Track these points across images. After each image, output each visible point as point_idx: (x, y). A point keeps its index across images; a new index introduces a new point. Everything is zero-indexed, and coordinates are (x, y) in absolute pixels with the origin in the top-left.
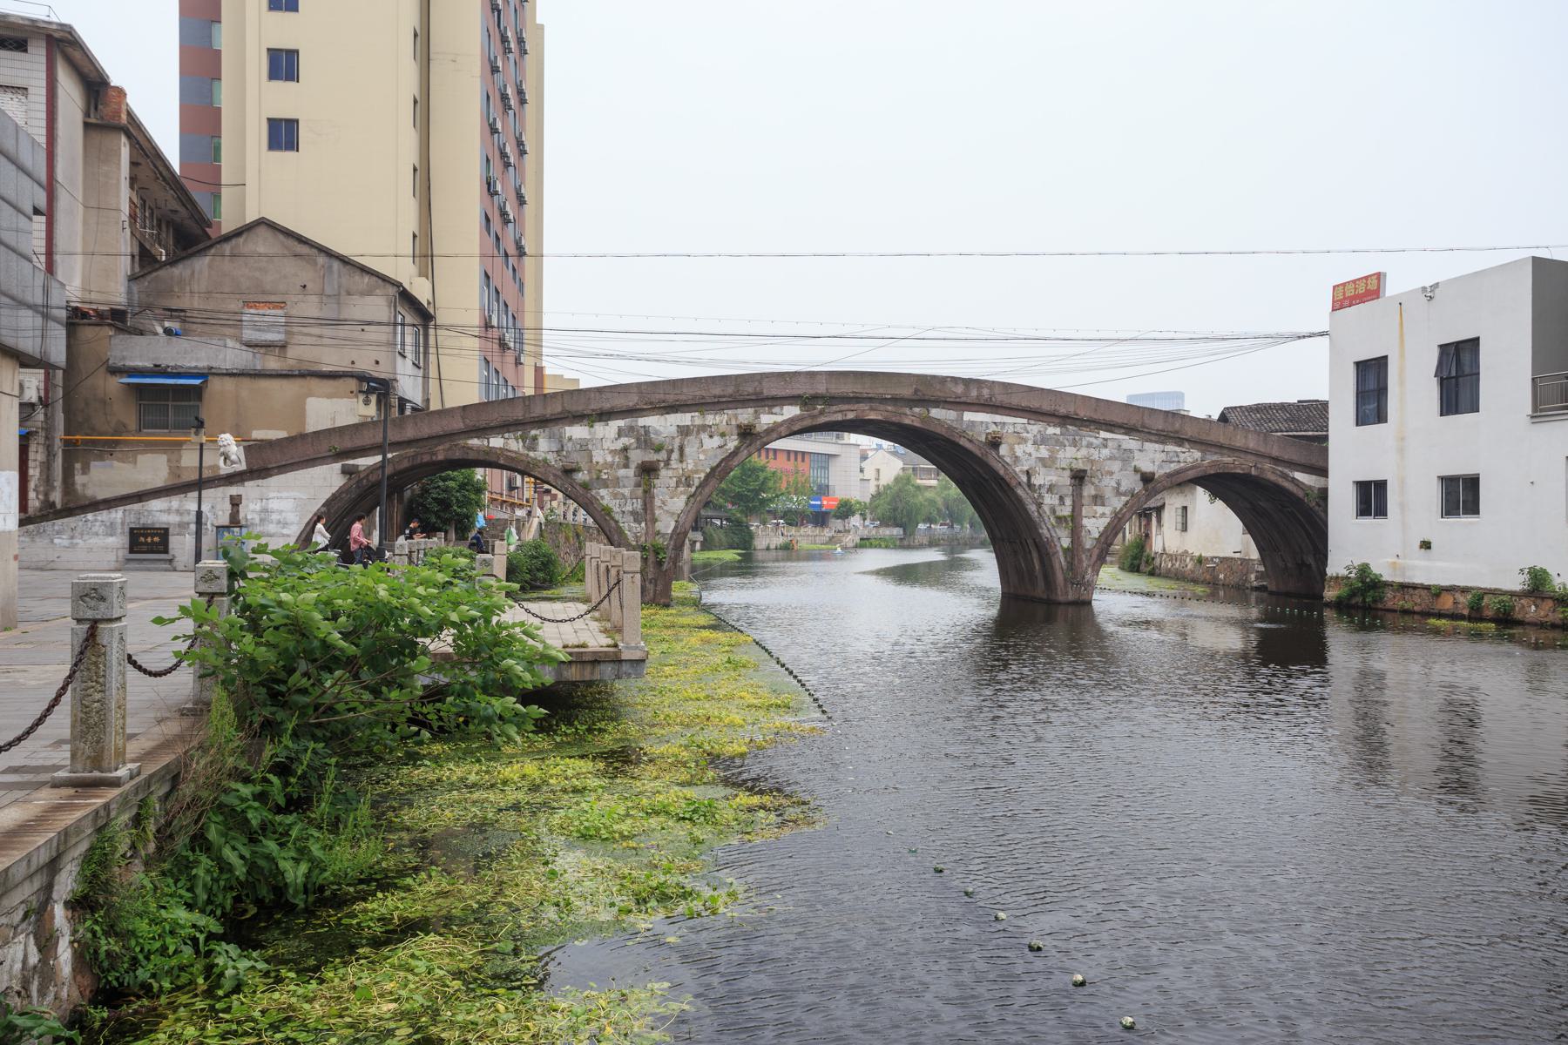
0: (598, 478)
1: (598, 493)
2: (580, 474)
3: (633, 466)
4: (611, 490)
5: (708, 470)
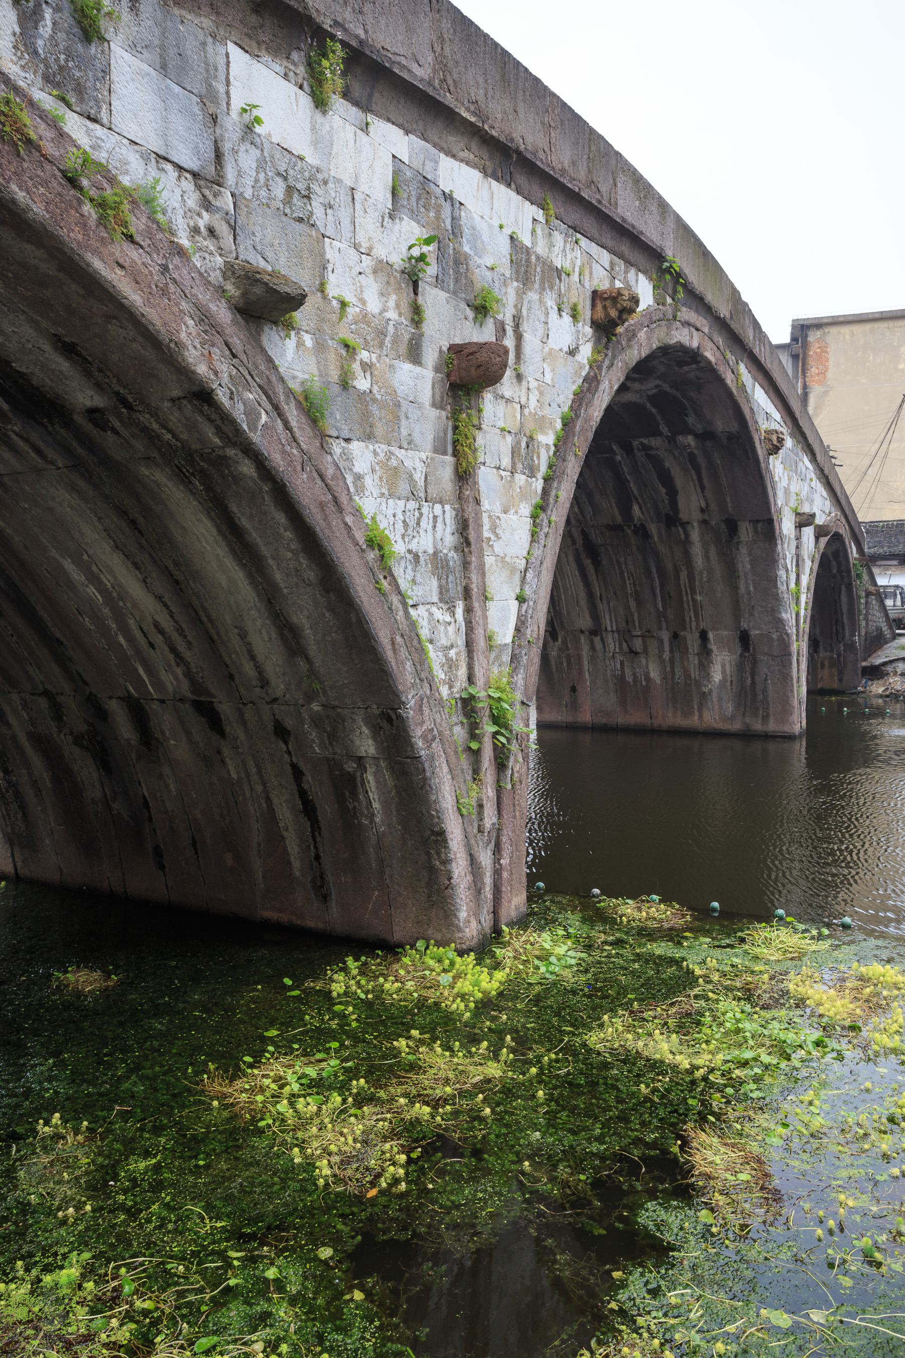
0: (345, 385)
1: (348, 457)
2: (291, 344)
3: (431, 356)
4: (382, 448)
5: (559, 425)
